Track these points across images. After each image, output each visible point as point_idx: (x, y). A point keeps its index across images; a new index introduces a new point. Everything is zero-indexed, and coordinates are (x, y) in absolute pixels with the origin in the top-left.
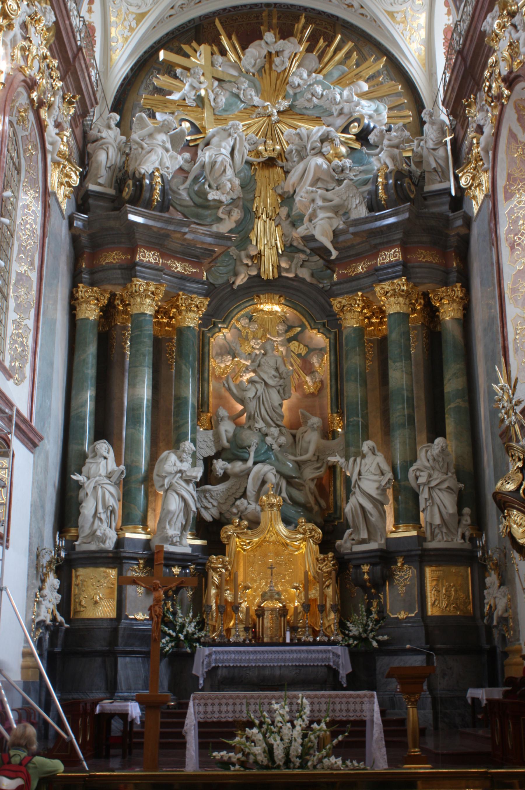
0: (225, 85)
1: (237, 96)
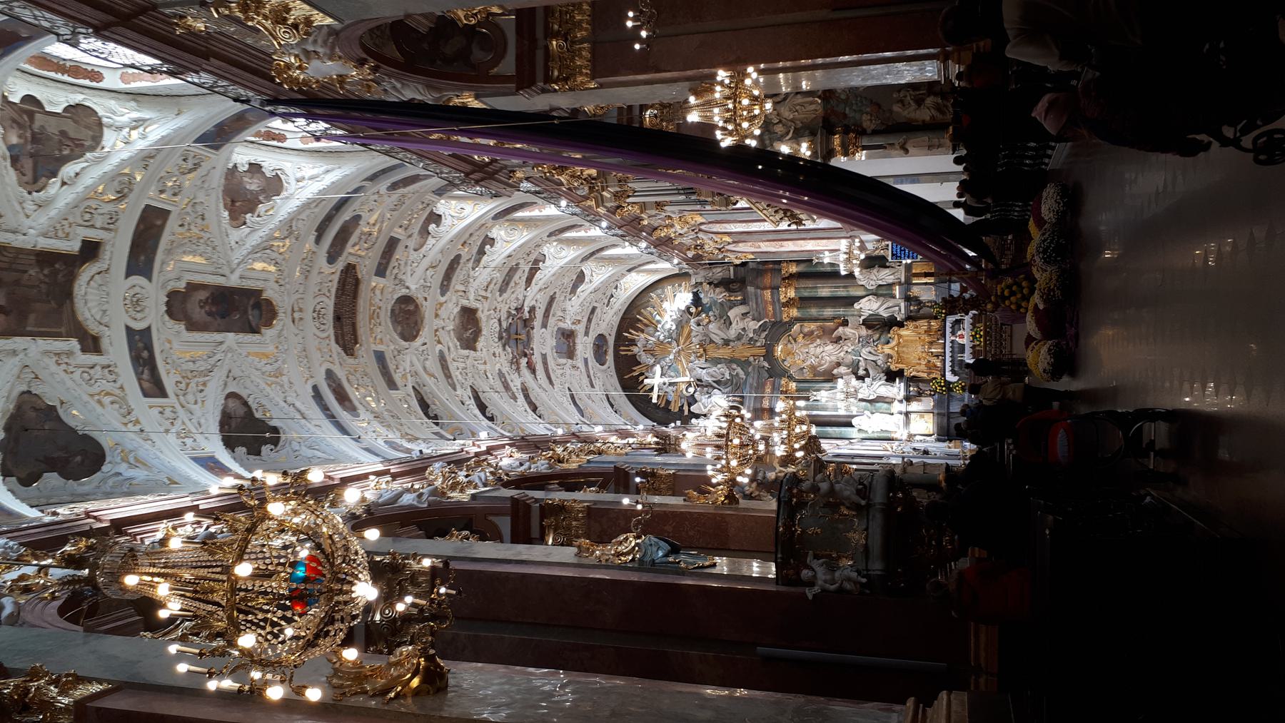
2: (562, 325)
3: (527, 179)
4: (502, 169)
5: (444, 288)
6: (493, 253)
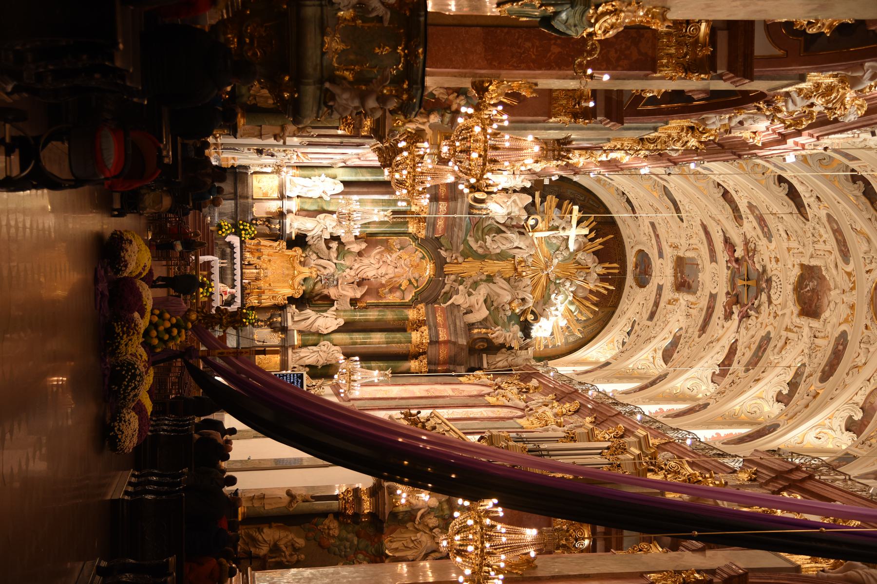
0: (564, 243)
1: (558, 250)
2: (691, 298)
3: (735, 471)
4: (767, 483)
5: (842, 341)
6: (779, 384)
